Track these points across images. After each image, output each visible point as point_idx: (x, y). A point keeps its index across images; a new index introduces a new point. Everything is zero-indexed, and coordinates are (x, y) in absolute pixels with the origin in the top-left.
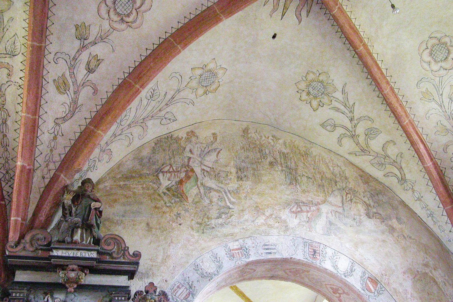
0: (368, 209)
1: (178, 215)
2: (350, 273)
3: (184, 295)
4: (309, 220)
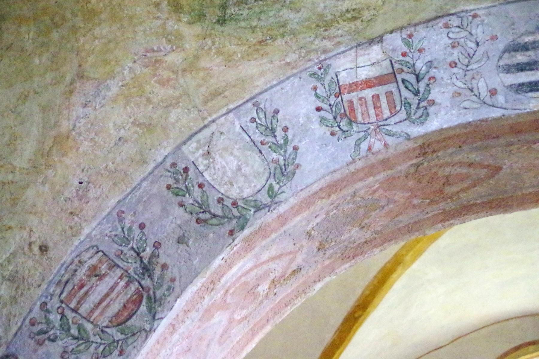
3: (116, 307)
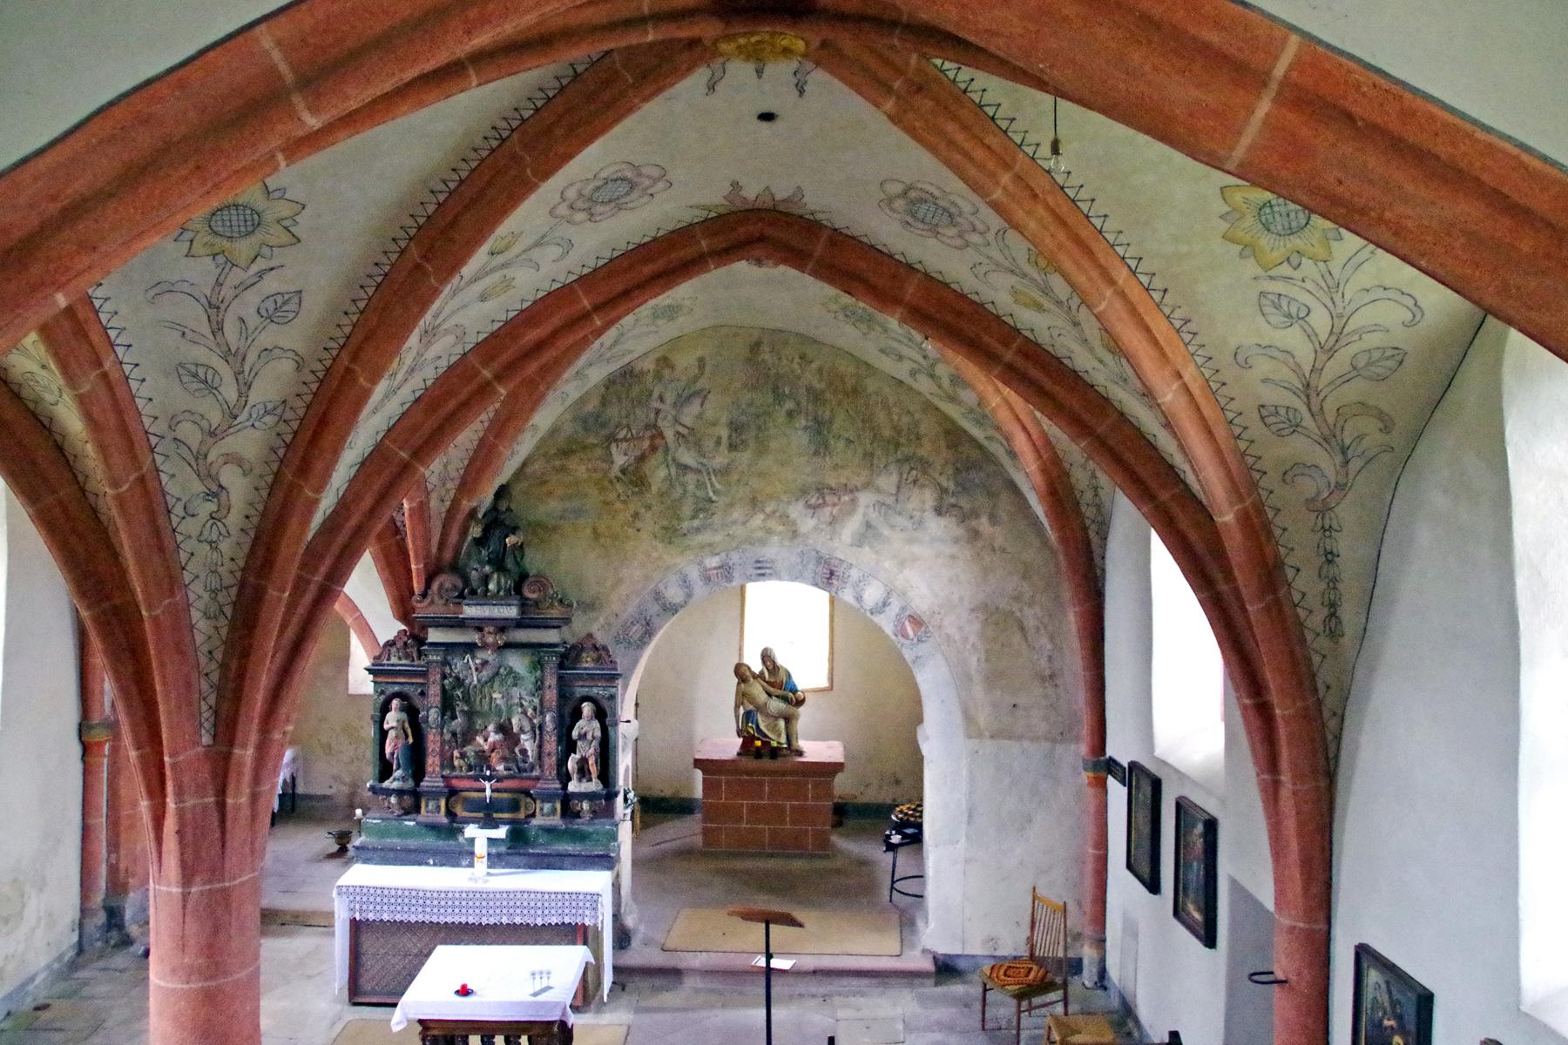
0: (941, 498)
1: (636, 515)
4: (833, 521)
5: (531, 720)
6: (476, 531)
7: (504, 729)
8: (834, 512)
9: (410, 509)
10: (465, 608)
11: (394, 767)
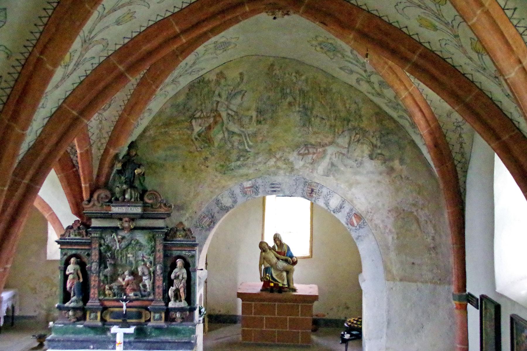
0: (373, 150)
1: (206, 159)
2: (339, 209)
3: (208, 223)
5: (148, 268)
6: (118, 166)
7: (133, 273)
8: (314, 158)
9: (81, 154)
10: (113, 208)
11: (72, 295)
